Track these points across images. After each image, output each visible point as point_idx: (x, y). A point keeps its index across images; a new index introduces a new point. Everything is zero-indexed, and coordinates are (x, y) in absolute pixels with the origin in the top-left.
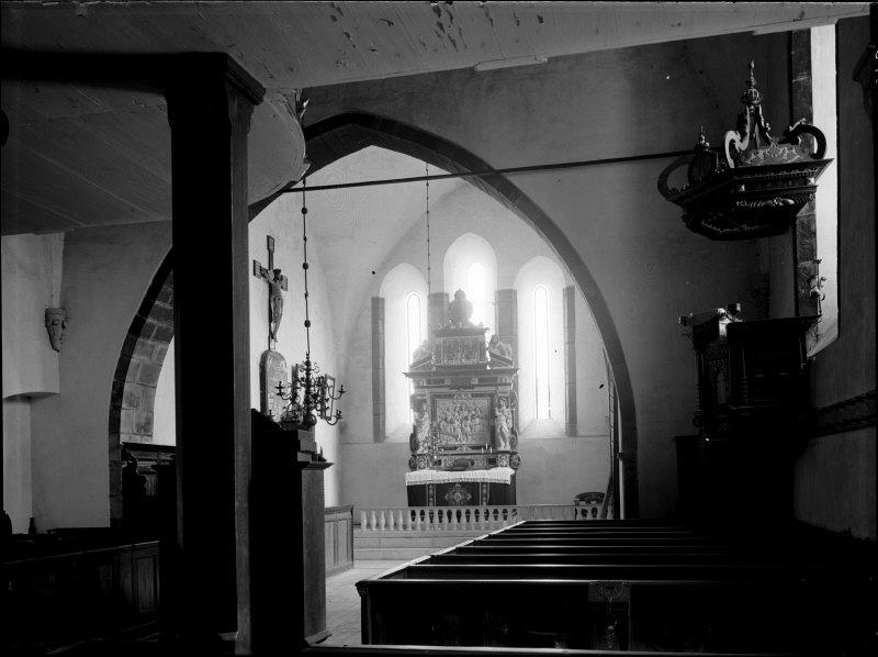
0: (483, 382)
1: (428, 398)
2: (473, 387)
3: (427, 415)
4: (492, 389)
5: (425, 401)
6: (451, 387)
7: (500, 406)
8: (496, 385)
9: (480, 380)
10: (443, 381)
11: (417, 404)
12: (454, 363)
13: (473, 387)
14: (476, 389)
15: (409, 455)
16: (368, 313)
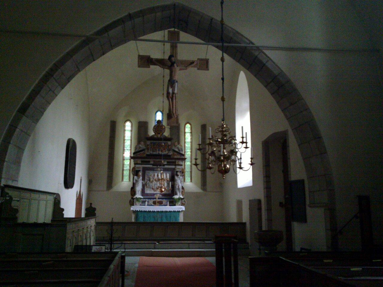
0: (169, 163)
1: (141, 169)
2: (164, 165)
3: (141, 178)
4: (173, 167)
5: (139, 171)
6: (153, 165)
7: (177, 175)
8: (176, 165)
9: (168, 162)
10: (149, 162)
11: (135, 172)
12: (155, 153)
13: (164, 165)
14: (166, 166)
15: (130, 197)
16: (108, 127)
